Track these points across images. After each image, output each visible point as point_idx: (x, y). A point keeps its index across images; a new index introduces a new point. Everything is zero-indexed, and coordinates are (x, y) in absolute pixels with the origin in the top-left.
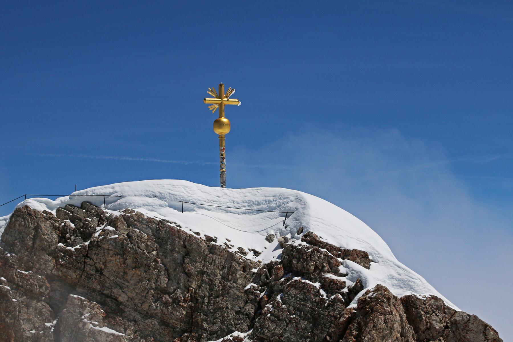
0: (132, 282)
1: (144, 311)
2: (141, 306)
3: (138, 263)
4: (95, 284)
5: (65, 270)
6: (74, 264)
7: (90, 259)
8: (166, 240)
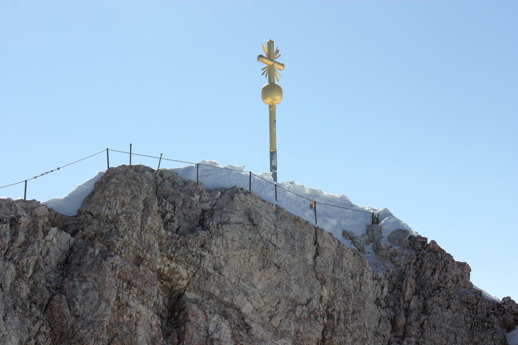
0: (259, 287)
1: (274, 327)
2: (270, 320)
3: (267, 262)
4: (213, 287)
5: (173, 265)
6: (187, 257)
7: (208, 251)
8: (291, 233)
